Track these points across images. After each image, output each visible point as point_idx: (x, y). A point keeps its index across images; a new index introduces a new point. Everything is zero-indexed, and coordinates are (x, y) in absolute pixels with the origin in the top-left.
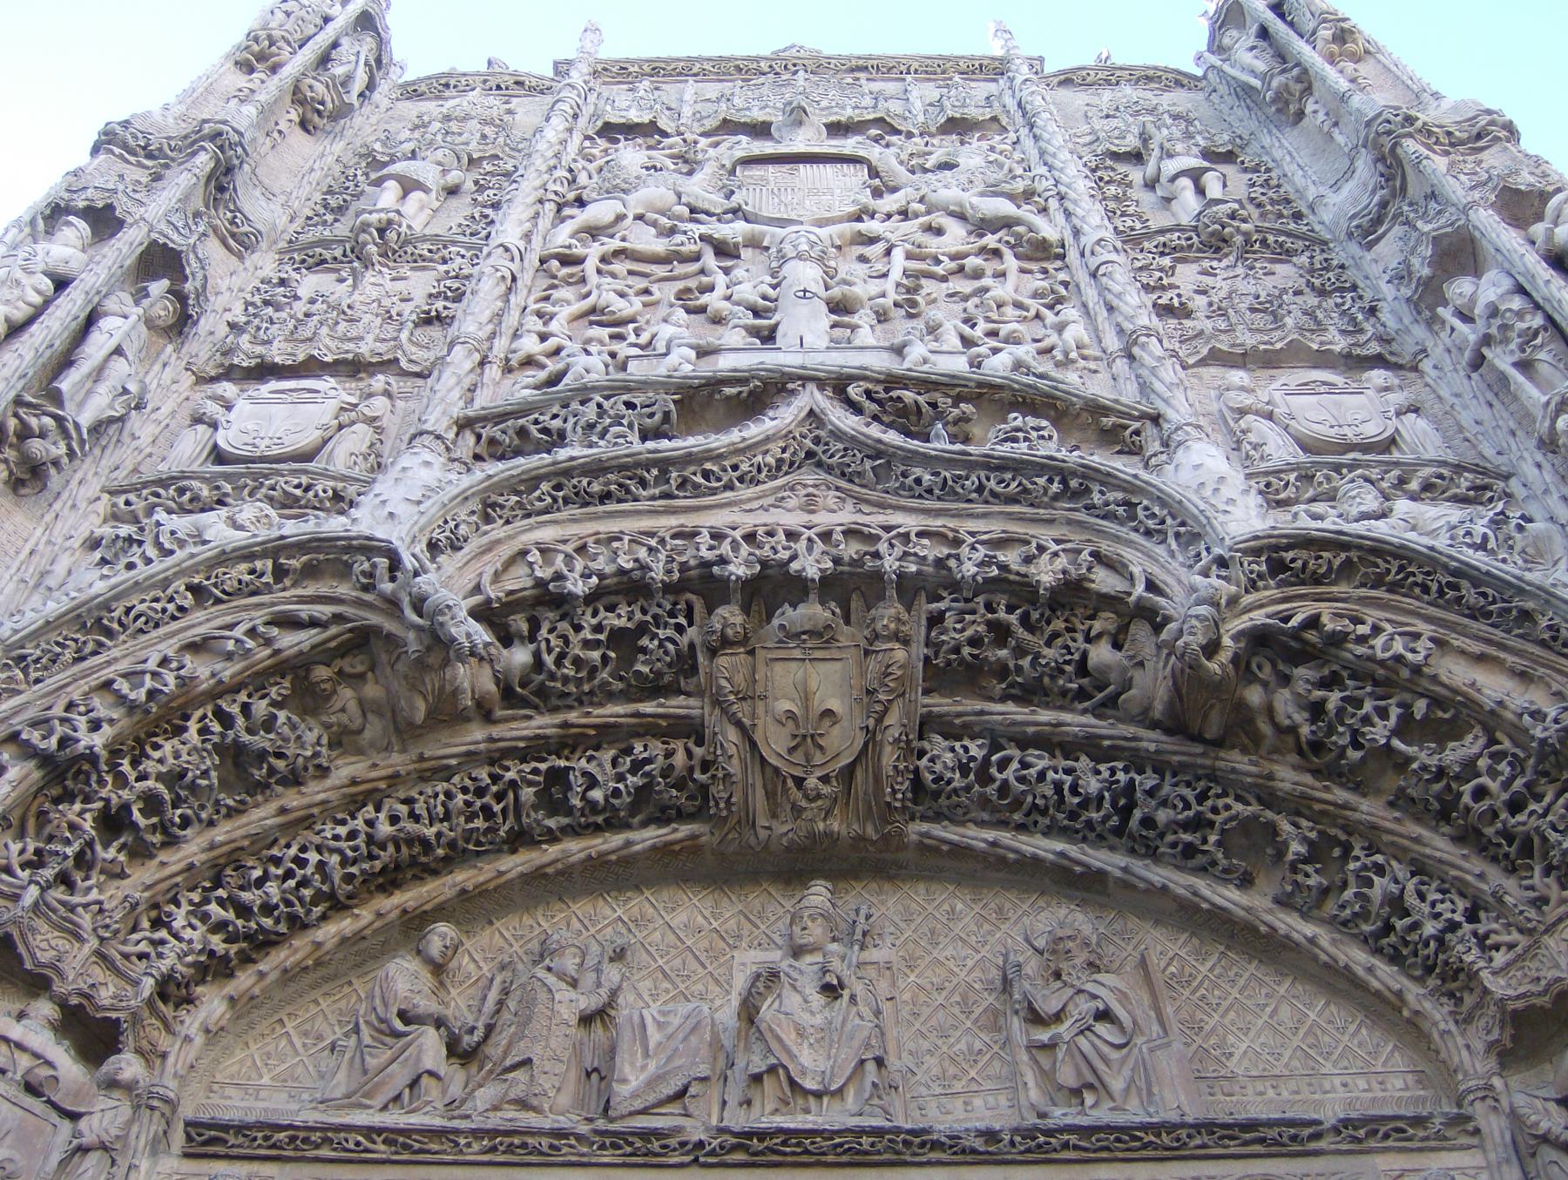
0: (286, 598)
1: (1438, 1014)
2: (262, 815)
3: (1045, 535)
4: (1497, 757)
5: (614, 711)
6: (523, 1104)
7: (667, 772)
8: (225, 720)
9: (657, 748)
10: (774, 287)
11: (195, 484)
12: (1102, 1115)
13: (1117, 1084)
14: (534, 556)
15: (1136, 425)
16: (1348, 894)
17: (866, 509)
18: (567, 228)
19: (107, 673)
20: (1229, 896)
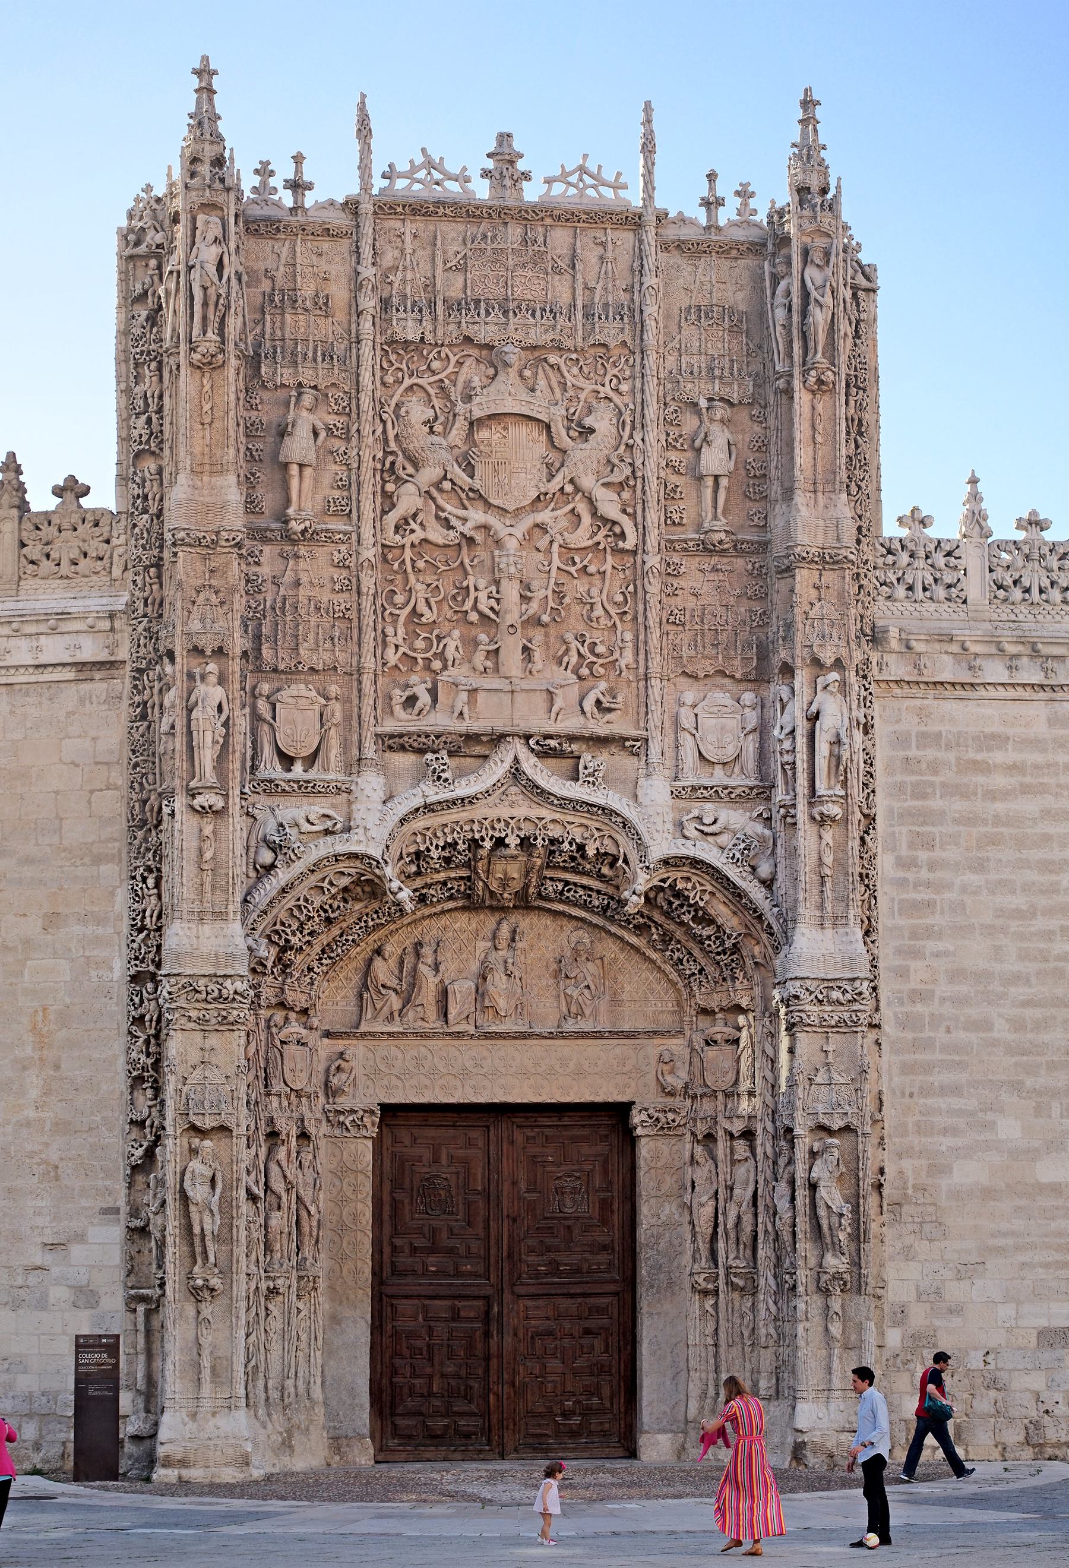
0: (340, 867)
1: (685, 993)
2: (336, 931)
3: (593, 825)
4: (717, 938)
5: (442, 876)
6: (423, 1019)
7: (458, 891)
8: (326, 911)
9: (456, 884)
10: (498, 600)
11: (282, 784)
12: (585, 1025)
13: (587, 1012)
14: (419, 839)
15: (638, 744)
16: (668, 953)
17: (534, 805)
18: (392, 518)
19: (289, 906)
20: (633, 940)
